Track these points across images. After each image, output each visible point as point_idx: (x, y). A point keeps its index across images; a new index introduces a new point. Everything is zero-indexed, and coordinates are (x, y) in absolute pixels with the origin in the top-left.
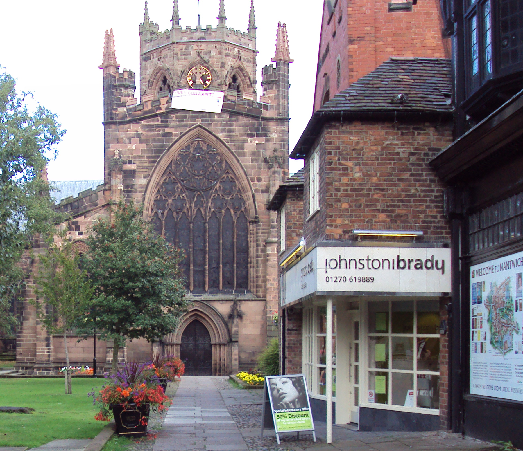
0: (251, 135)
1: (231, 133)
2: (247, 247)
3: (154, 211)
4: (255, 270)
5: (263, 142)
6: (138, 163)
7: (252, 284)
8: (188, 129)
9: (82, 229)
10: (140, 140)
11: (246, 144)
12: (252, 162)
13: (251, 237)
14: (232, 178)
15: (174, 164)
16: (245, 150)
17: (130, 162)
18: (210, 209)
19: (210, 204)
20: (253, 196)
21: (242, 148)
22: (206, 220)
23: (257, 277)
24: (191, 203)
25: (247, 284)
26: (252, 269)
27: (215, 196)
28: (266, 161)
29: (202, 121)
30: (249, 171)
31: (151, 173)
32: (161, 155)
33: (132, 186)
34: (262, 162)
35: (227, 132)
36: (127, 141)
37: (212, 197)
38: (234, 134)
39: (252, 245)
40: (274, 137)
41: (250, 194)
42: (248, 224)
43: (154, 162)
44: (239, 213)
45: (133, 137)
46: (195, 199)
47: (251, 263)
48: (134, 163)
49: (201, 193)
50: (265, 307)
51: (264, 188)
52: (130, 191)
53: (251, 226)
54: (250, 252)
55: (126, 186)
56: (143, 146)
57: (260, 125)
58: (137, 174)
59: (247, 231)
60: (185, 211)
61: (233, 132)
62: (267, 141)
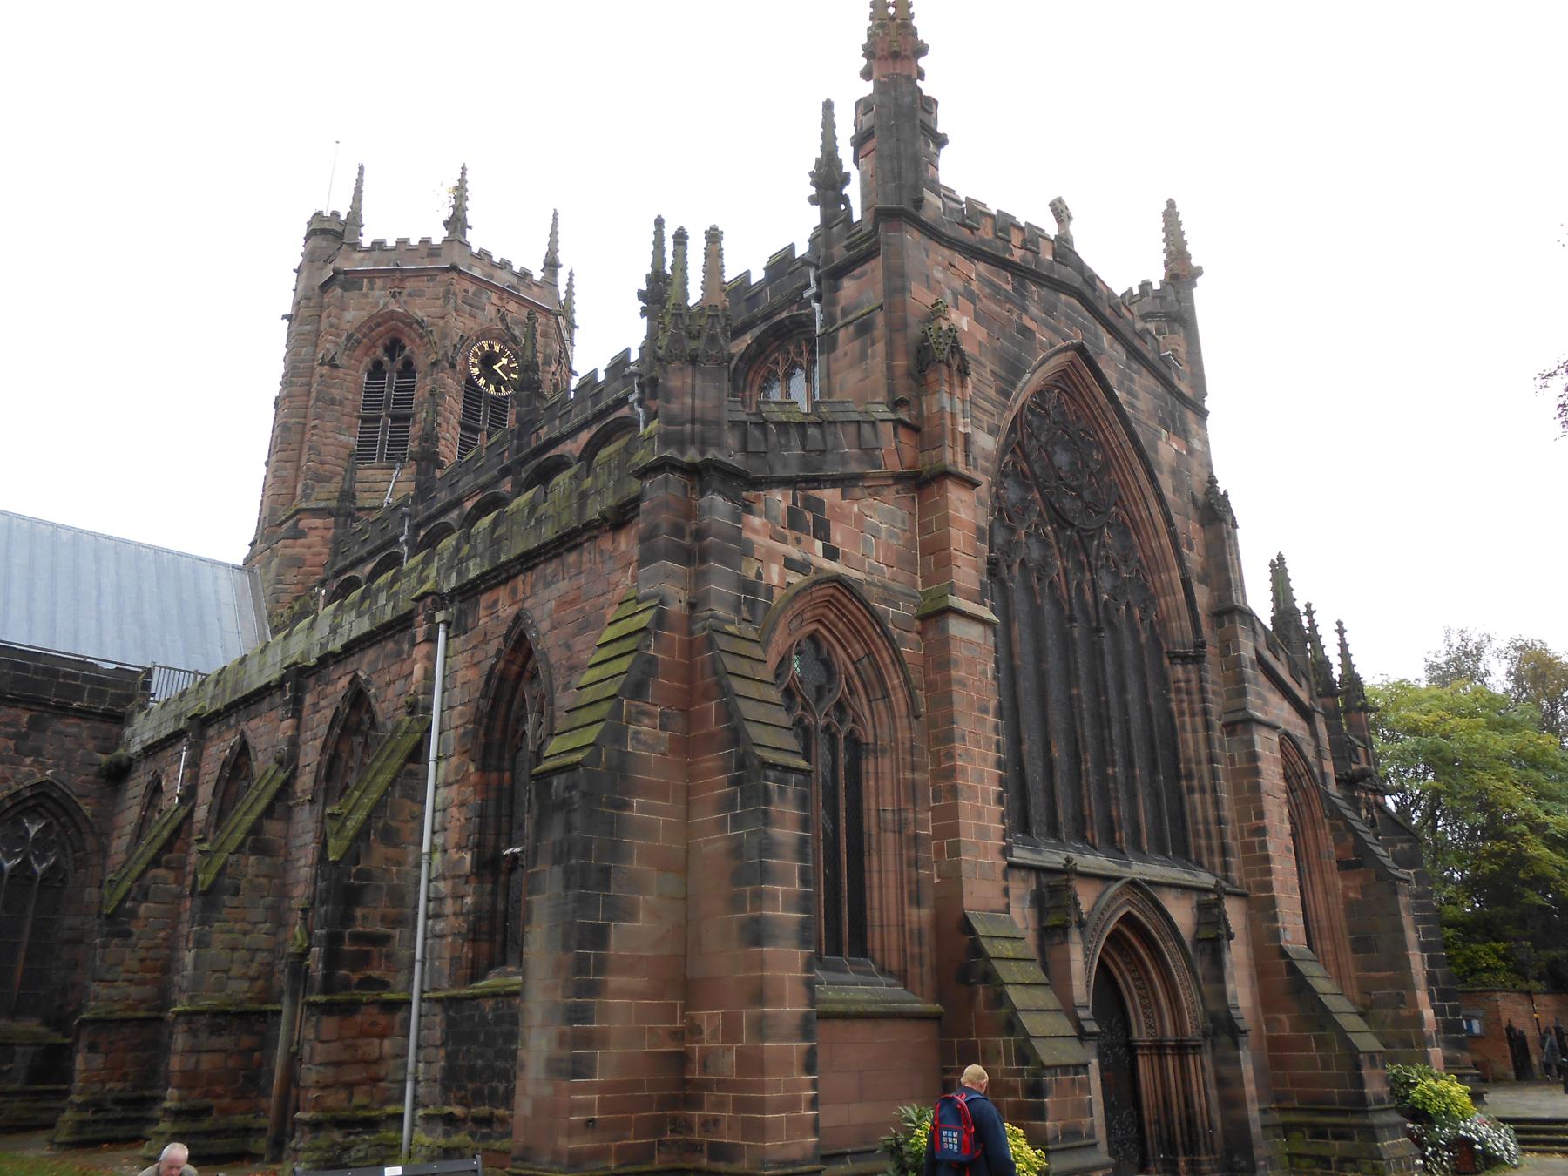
4: (1208, 797)
9: (837, 538)
13: (1182, 701)
26: (1197, 796)
41: (1176, 575)
42: (1166, 662)
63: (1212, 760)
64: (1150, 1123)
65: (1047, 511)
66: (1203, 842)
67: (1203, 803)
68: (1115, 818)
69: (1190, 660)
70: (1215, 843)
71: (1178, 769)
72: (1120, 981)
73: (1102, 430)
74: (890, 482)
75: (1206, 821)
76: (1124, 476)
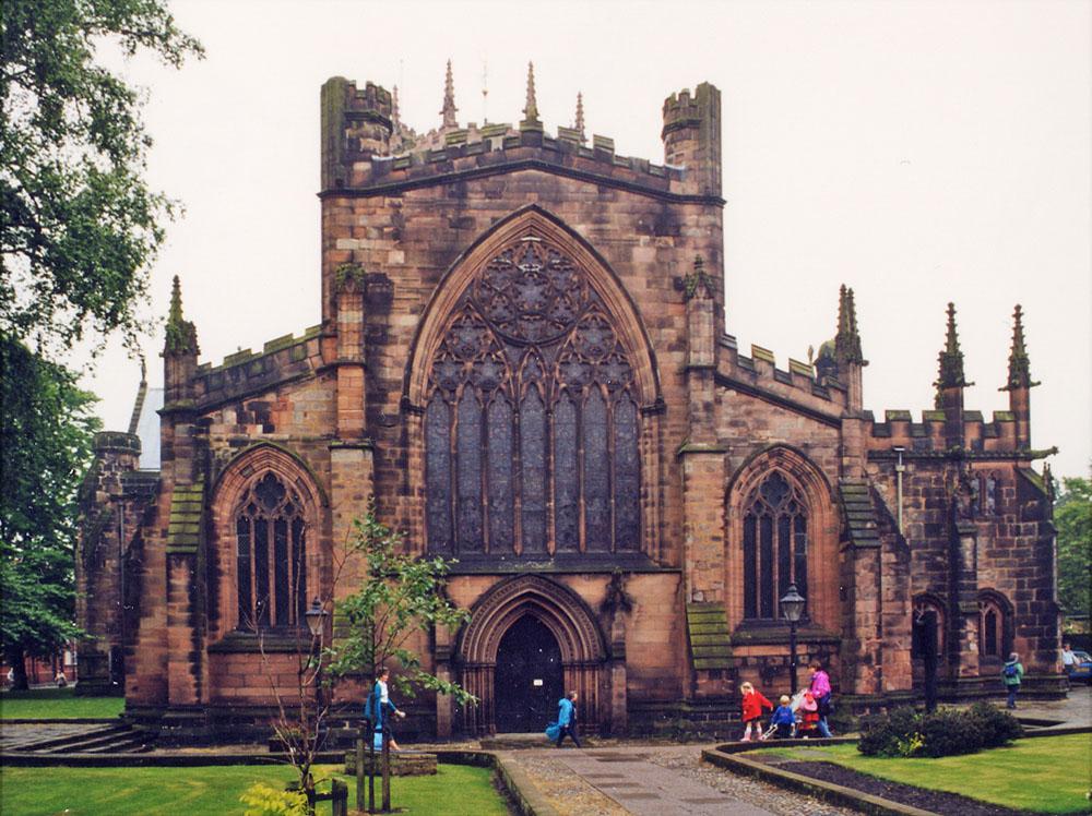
2: (640, 465)
3: (435, 386)
4: (655, 509)
7: (649, 540)
8: (509, 213)
12: (649, 284)
13: (646, 443)
14: (602, 320)
16: (633, 263)
18: (557, 383)
19: (557, 374)
21: (629, 258)
22: (549, 405)
24: (515, 372)
25: (638, 540)
26: (648, 509)
27: (567, 357)
29: (541, 199)
30: (643, 307)
31: (427, 303)
37: (561, 360)
38: (609, 226)
39: (650, 459)
41: (644, 352)
42: (639, 416)
46: (525, 362)
49: (536, 349)
50: (681, 584)
53: (646, 419)
54: (644, 474)
59: (638, 431)
60: (504, 387)
61: (608, 222)
63: (661, 483)
67: (652, 513)
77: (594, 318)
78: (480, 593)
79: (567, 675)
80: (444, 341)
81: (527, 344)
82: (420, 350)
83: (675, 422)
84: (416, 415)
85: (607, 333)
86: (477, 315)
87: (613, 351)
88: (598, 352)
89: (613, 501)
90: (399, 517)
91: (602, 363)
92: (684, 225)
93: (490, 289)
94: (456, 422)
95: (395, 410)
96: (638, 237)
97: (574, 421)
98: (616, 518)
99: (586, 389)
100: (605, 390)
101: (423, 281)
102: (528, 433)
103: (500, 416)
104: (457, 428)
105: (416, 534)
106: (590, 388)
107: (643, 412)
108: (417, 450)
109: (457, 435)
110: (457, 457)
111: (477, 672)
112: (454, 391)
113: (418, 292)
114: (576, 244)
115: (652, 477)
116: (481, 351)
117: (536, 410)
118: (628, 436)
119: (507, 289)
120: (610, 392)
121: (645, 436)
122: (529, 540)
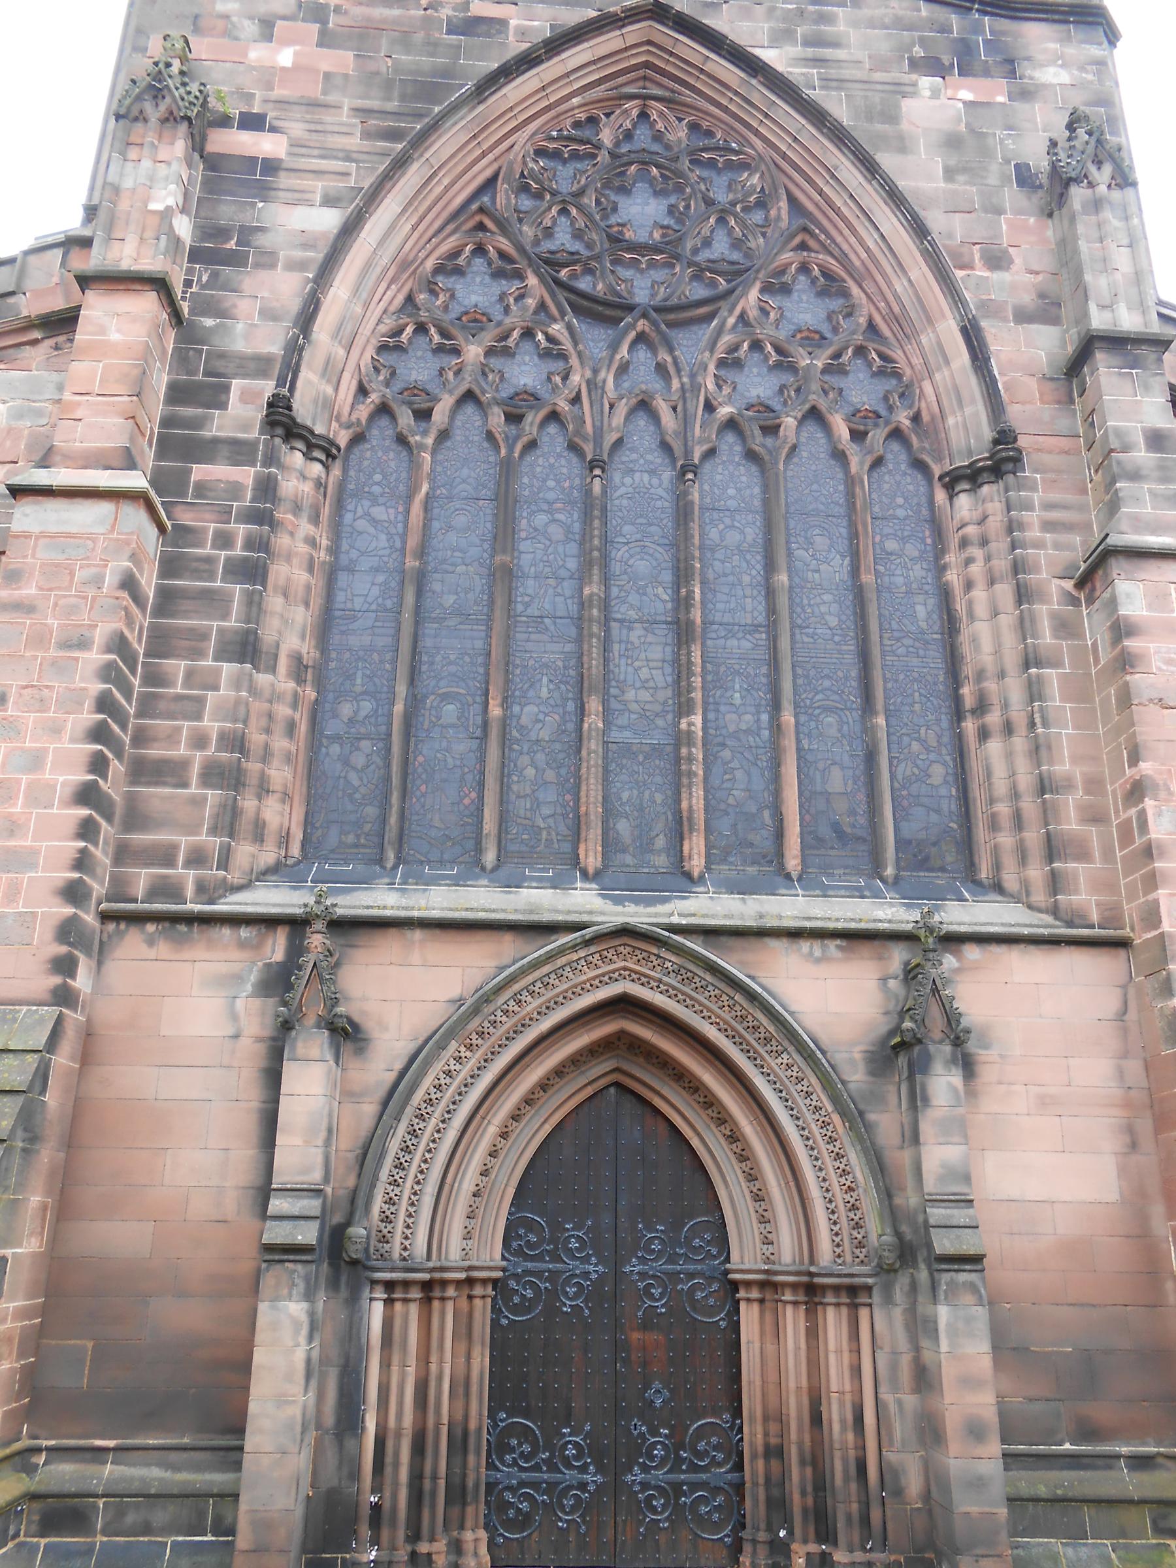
0: (935, 67)
1: (827, 52)
3: (374, 397)
4: (1019, 742)
5: (1001, 99)
6: (297, 129)
7: (1006, 839)
10: (323, 33)
11: (907, 105)
12: (950, 174)
13: (969, 561)
15: (507, 180)
16: (904, 126)
17: (253, 122)
18: (709, 407)
19: (711, 385)
20: (972, 336)
21: (891, 116)
22: (688, 453)
23: (1043, 786)
25: (967, 845)
26: (994, 746)
27: (735, 348)
28: (1024, 177)
30: (935, 220)
31: (366, 184)
32: (437, 109)
33: (247, 233)
34: (1005, 179)
35: (807, 43)
36: (250, 28)
37: (719, 353)
38: (840, 54)
40: (1055, 81)
41: (949, 329)
42: (940, 496)
43: (393, 135)
44: (877, 436)
45: (284, 18)
46: (624, 351)
47: (982, 707)
48: (273, 129)
51: (1027, 299)
52: (236, 259)
54: (966, 649)
55: (211, 231)
56: (342, 60)
57: (978, 29)
58: (284, 180)
60: (563, 406)
61: (836, 45)
62: (1025, 94)
63: (1030, 660)
64: (754, 1456)
65: (553, 296)
66: (1006, 839)
67: (1009, 755)
68: (685, 814)
69: (985, 476)
70: (1033, 836)
71: (957, 700)
72: (695, 1142)
73: (757, 133)
74: (36, 334)
75: (1015, 795)
76: (821, 193)
77: (804, 268)
78: (455, 993)
79: (750, 1317)
80: (410, 299)
81: (630, 308)
82: (339, 293)
83: (1055, 496)
84: (308, 457)
85: (836, 304)
86: (505, 244)
87: (859, 338)
88: (814, 339)
89: (881, 721)
90: (212, 725)
91: (827, 369)
92: (1028, 59)
93: (538, 196)
94: (425, 488)
95: (246, 427)
96: (914, 77)
97: (757, 503)
98: (893, 777)
99: (789, 422)
100: (842, 430)
101: (367, 135)
102: (627, 529)
103: (551, 483)
104: (427, 507)
105: (263, 789)
106: (801, 422)
107: (951, 482)
108: (303, 548)
109: (426, 527)
110: (421, 580)
111: (427, 1301)
112: (423, 415)
113: (348, 158)
114: (759, 92)
115: (997, 652)
116: (508, 321)
117: (652, 473)
118: (912, 550)
119: (581, 192)
120: (852, 432)
121: (964, 543)
122: (623, 827)
